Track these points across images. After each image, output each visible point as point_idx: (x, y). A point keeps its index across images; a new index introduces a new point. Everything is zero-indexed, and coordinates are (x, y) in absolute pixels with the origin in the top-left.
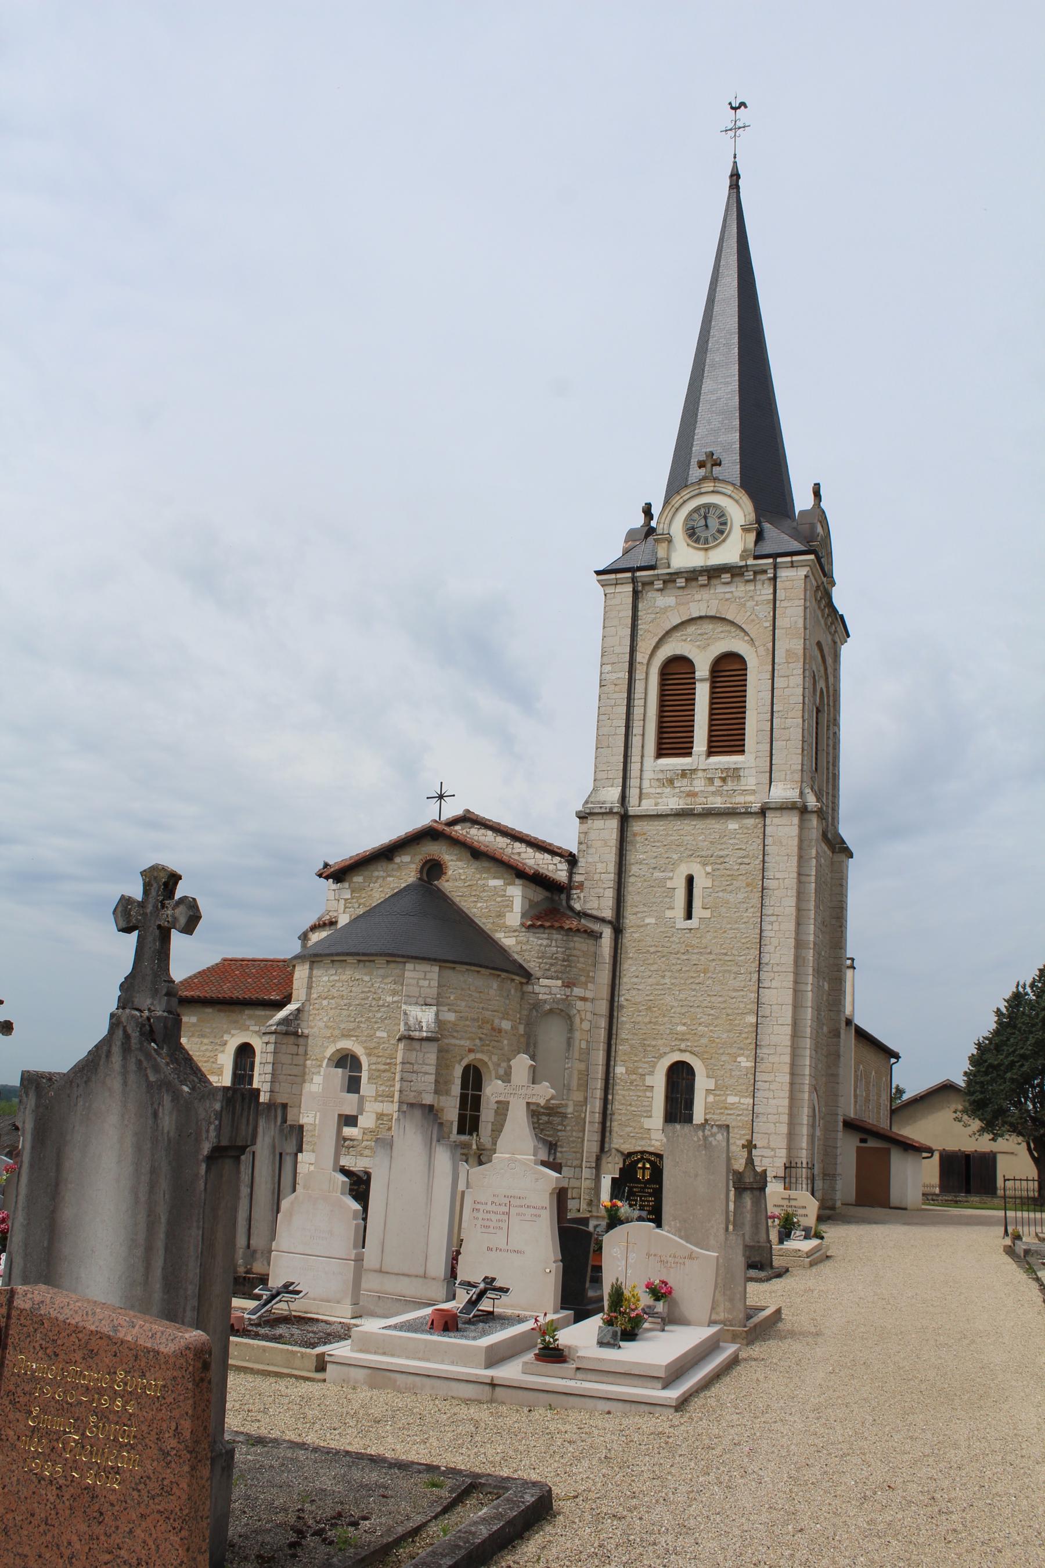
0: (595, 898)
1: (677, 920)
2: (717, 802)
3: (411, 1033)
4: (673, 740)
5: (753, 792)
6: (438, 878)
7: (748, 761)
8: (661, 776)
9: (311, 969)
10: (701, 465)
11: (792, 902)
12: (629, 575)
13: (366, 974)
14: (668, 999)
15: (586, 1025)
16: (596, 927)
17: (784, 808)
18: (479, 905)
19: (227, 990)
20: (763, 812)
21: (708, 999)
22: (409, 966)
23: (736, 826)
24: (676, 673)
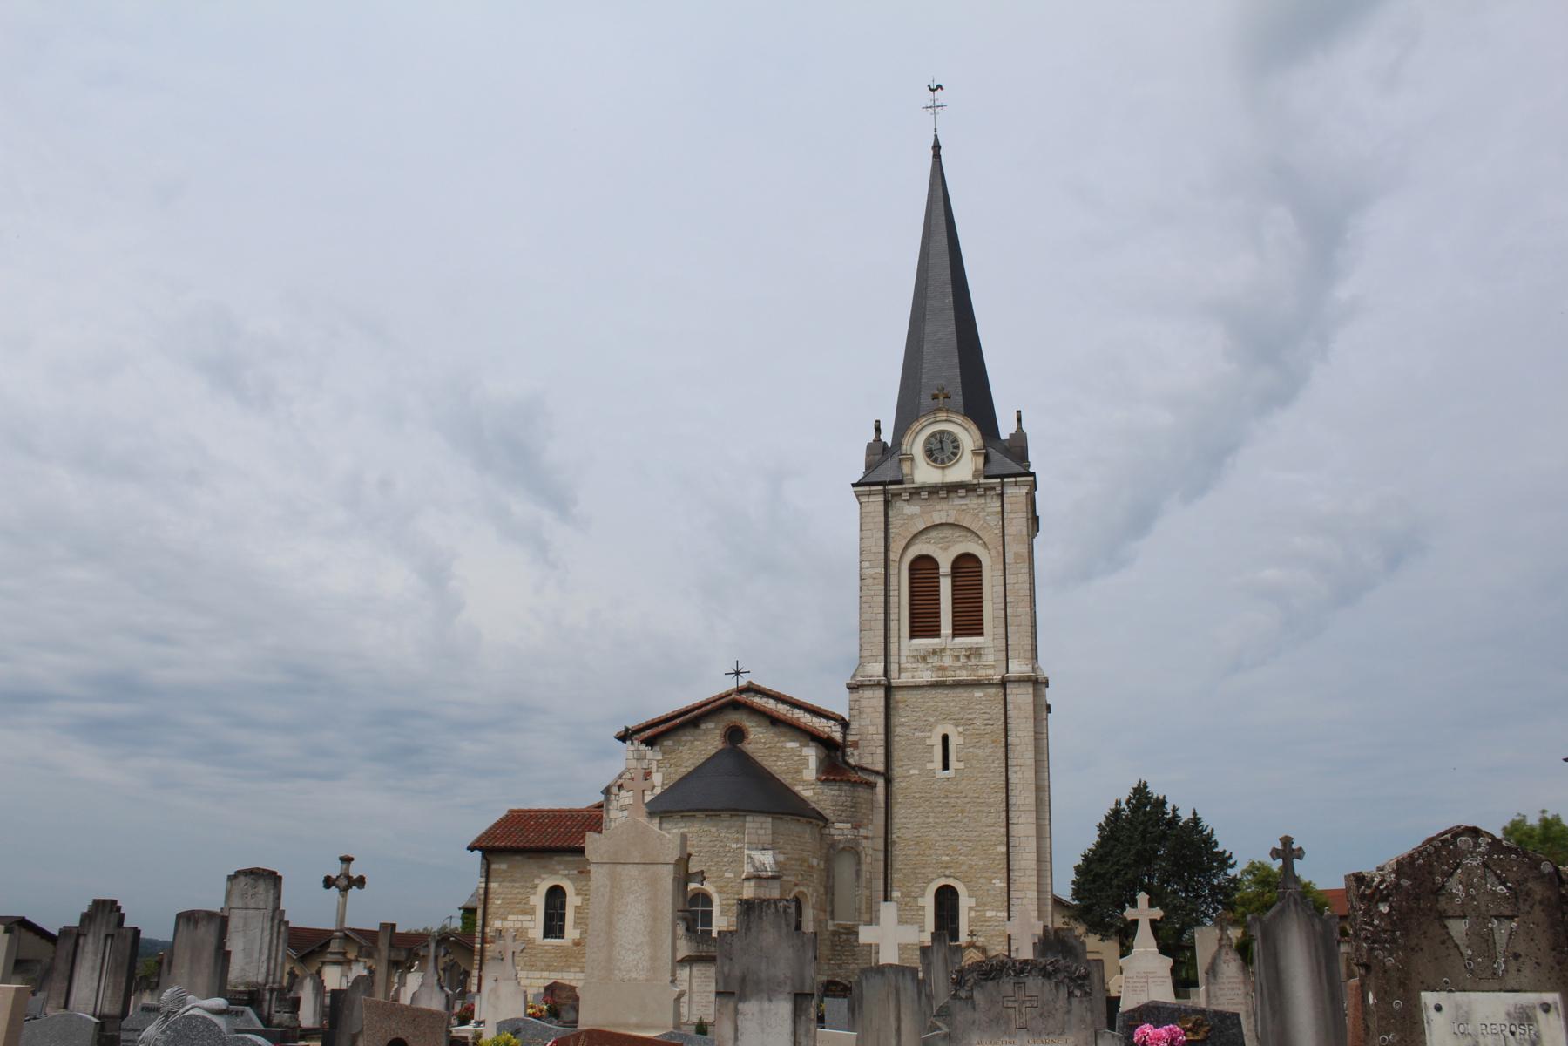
2: (963, 675)
4: (923, 624)
5: (993, 667)
11: (1031, 755)
14: (934, 835)
15: (869, 859)
16: (872, 778)
17: (1022, 680)
19: (533, 839)
20: (1004, 683)
22: (749, 818)
24: (923, 568)
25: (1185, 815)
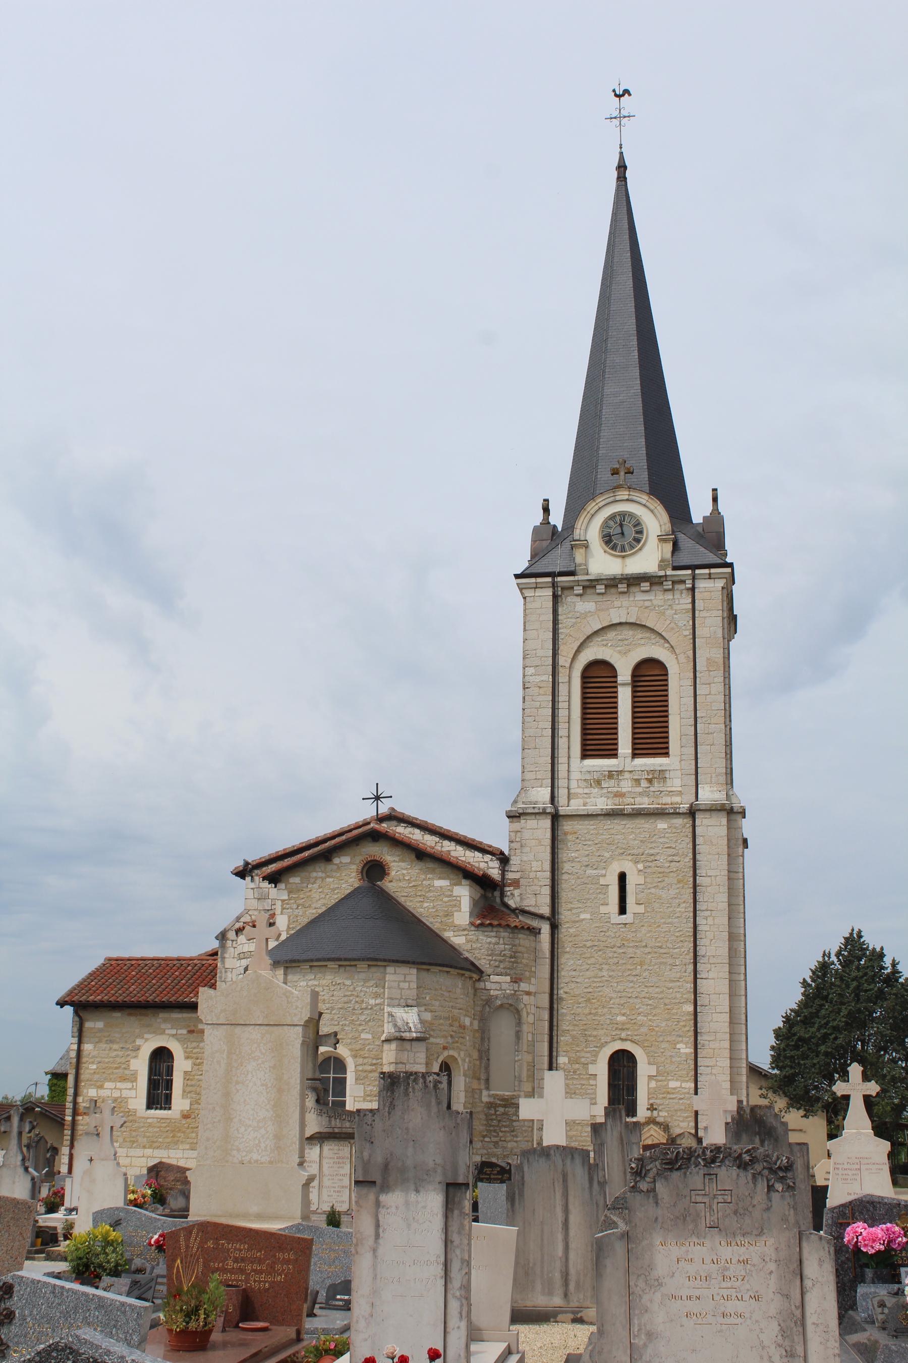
0: (531, 895)
1: (612, 916)
2: (645, 803)
3: (403, 1035)
4: (598, 741)
5: (680, 793)
6: (381, 879)
7: (675, 763)
8: (588, 777)
9: (285, 974)
11: (724, 898)
12: (549, 579)
13: (347, 979)
14: (607, 991)
15: (531, 1019)
16: (535, 923)
17: (714, 809)
18: (426, 905)
19: (134, 993)
20: (692, 813)
21: (646, 990)
22: (390, 970)
23: (665, 826)
24: (598, 676)
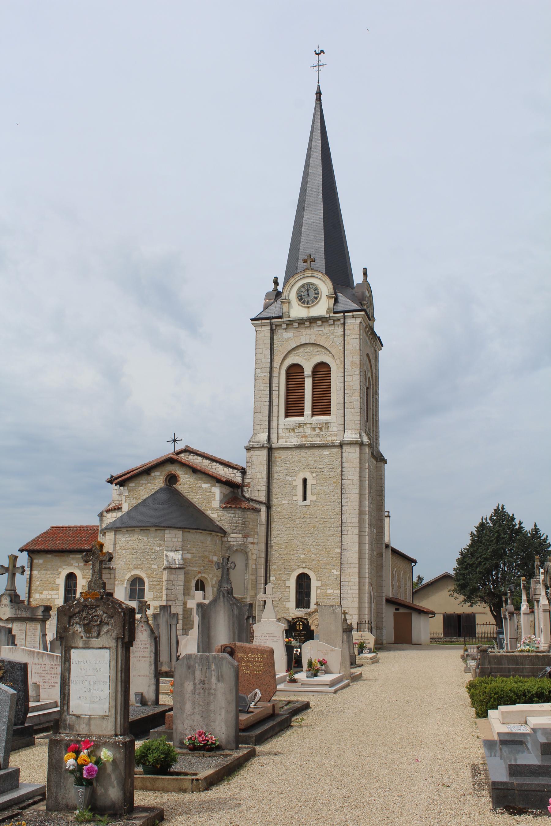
0: (256, 491)
1: (299, 502)
2: (317, 441)
3: (171, 566)
4: (294, 408)
5: (336, 435)
6: (175, 484)
7: (333, 419)
8: (288, 427)
9: (115, 535)
10: (305, 261)
12: (268, 321)
13: (145, 537)
14: (296, 541)
15: (254, 557)
16: (257, 506)
17: (352, 443)
18: (198, 497)
19: (58, 545)
20: (341, 445)
21: (316, 541)
23: (328, 453)
24: (295, 371)
25: (528, 527)
